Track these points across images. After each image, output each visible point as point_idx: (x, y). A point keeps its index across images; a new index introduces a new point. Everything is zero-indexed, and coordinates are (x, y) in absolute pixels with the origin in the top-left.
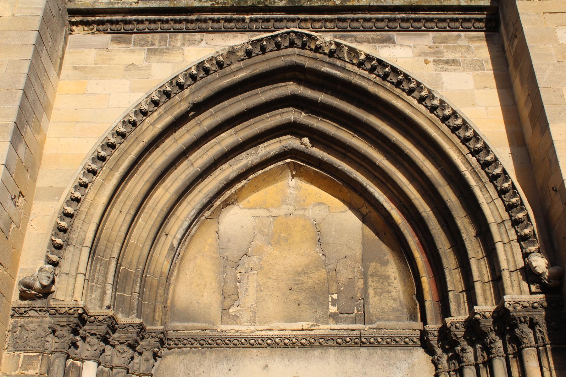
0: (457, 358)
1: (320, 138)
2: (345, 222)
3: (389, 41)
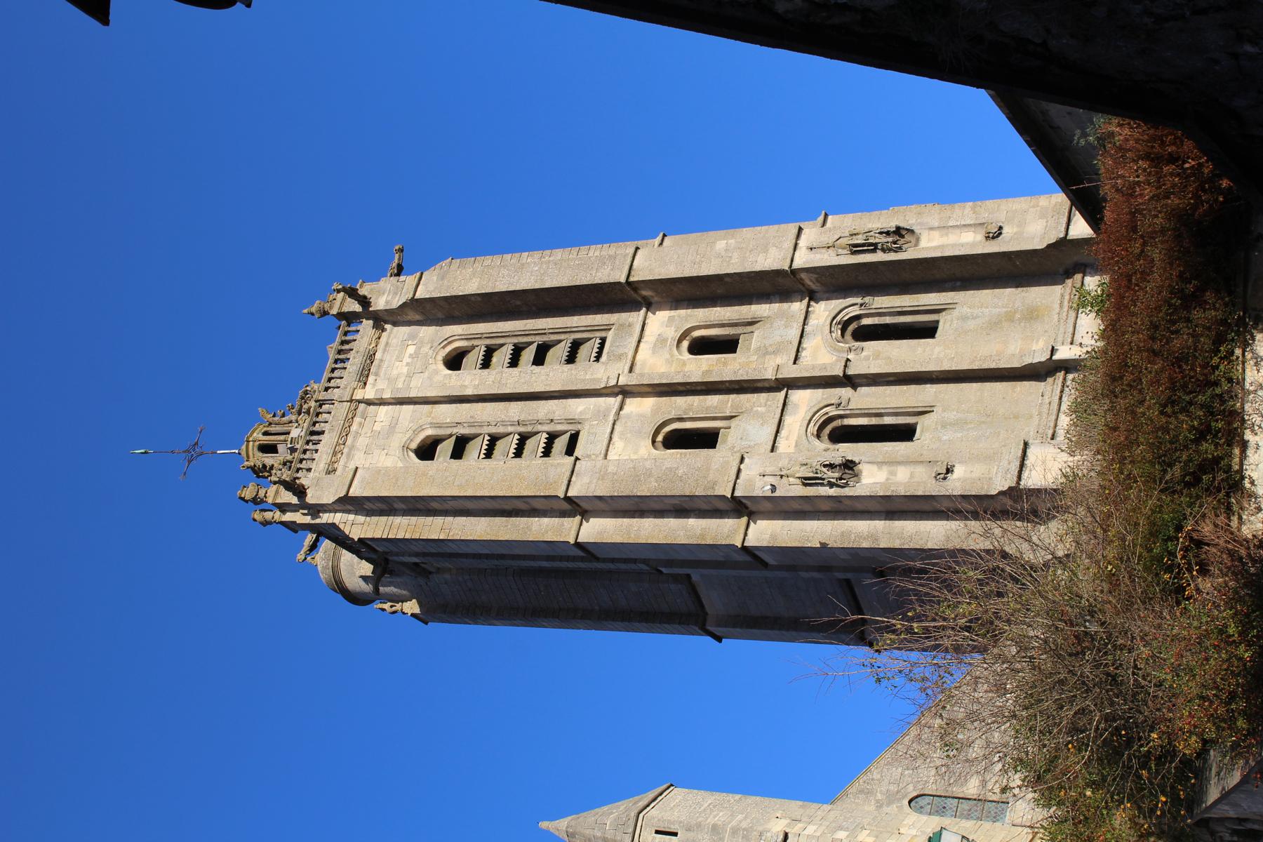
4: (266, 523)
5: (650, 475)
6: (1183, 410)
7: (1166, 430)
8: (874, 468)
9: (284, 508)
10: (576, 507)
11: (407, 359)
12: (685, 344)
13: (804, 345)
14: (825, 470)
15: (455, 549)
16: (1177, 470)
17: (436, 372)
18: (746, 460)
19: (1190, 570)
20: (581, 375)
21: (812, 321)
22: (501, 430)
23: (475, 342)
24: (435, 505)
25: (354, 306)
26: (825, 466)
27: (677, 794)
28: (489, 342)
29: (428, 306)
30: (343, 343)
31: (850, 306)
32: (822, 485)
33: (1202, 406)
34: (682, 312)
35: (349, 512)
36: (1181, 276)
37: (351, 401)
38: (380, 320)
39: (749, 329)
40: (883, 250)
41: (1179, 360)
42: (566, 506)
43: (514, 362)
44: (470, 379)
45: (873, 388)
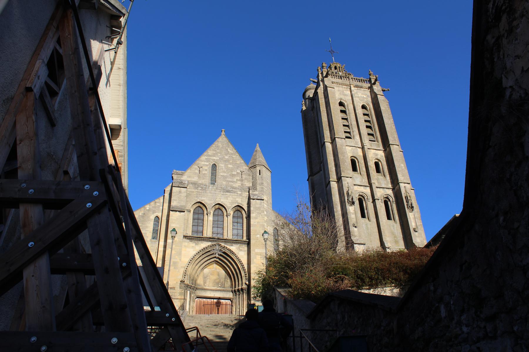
0: (236, 294)
1: (220, 259)
2: (223, 272)
3: (232, 245)
4: (318, 70)
6: (376, 273)
7: (370, 269)
9: (322, 73)
10: (333, 141)
12: (377, 161)
15: (319, 114)
16: (360, 273)
19: (335, 279)
20: (365, 137)
21: (387, 190)
22: (349, 120)
24: (328, 108)
25: (373, 82)
27: (269, 174)
31: (392, 198)
33: (378, 278)
36: (412, 268)
38: (371, 88)
41: (389, 270)
43: (366, 121)
44: (360, 111)
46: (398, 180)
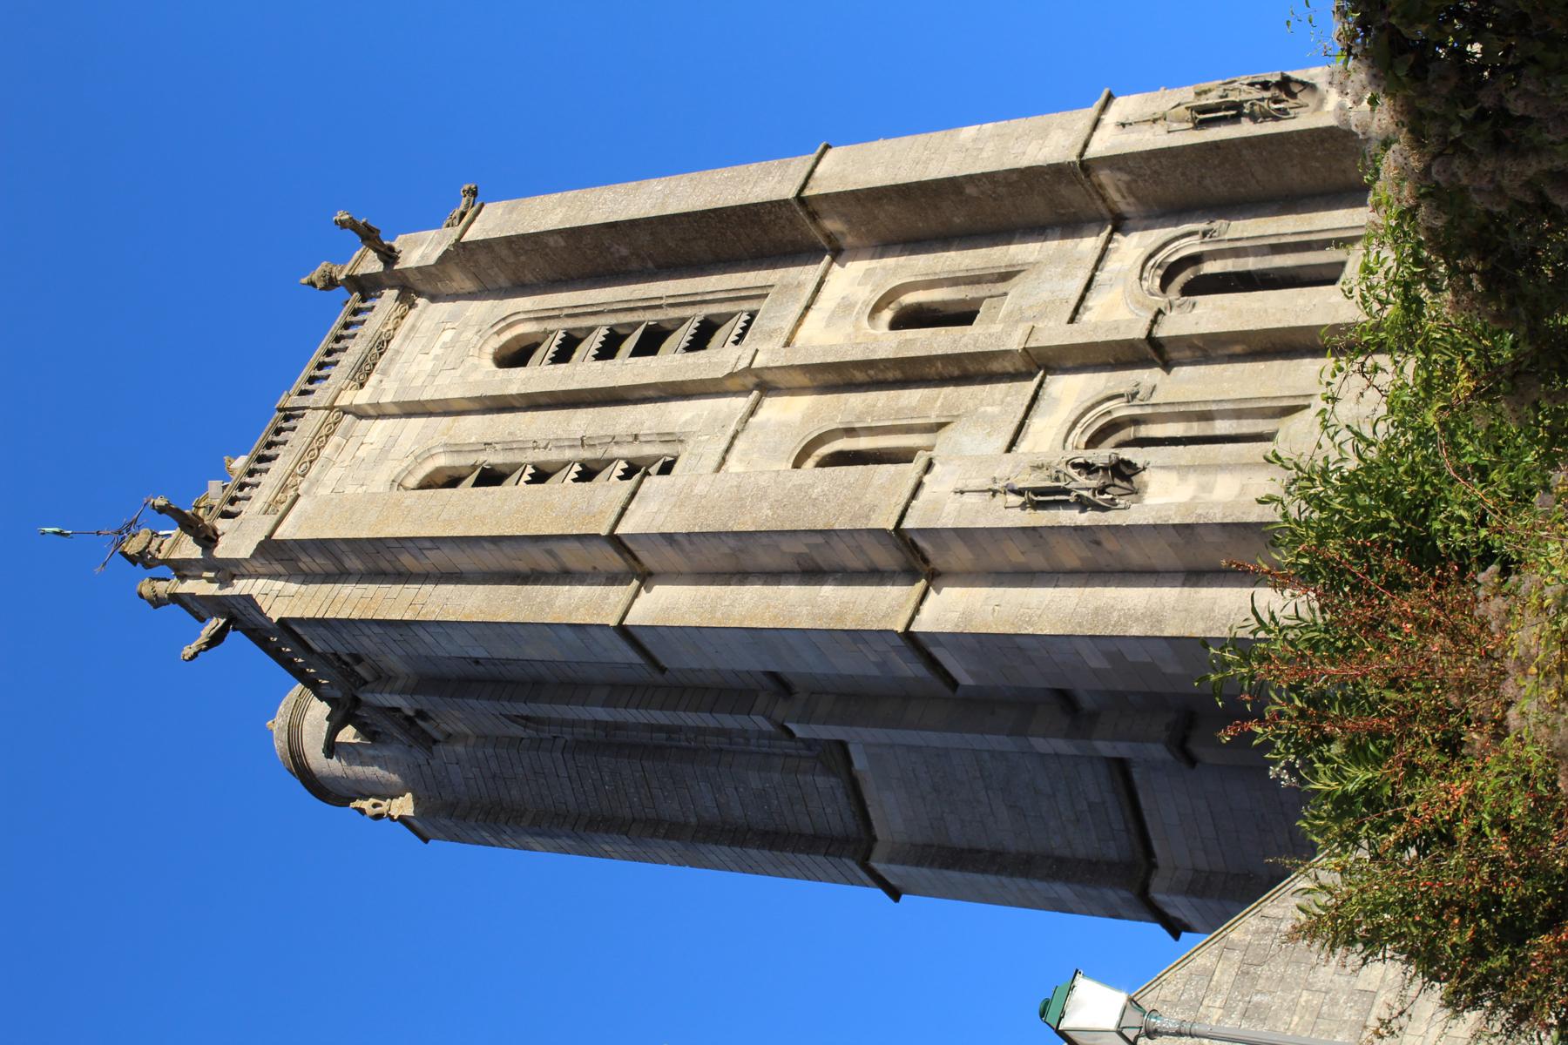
4: (157, 602)
5: (763, 497)
8: (1172, 478)
9: (182, 569)
10: (630, 561)
11: (437, 350)
12: (887, 315)
13: (1089, 303)
14: (1073, 472)
17: (476, 367)
18: (937, 469)
21: (1112, 264)
22: (554, 456)
23: (551, 325)
25: (372, 264)
26: (1075, 466)
28: (571, 324)
29: (483, 259)
30: (347, 326)
31: (1184, 238)
32: (1065, 504)
34: (890, 262)
35: (275, 576)
37: (331, 408)
38: (412, 287)
39: (1000, 287)
40: (1253, 117)
42: (616, 562)
45: (1202, 369)
46: (1057, 171)
